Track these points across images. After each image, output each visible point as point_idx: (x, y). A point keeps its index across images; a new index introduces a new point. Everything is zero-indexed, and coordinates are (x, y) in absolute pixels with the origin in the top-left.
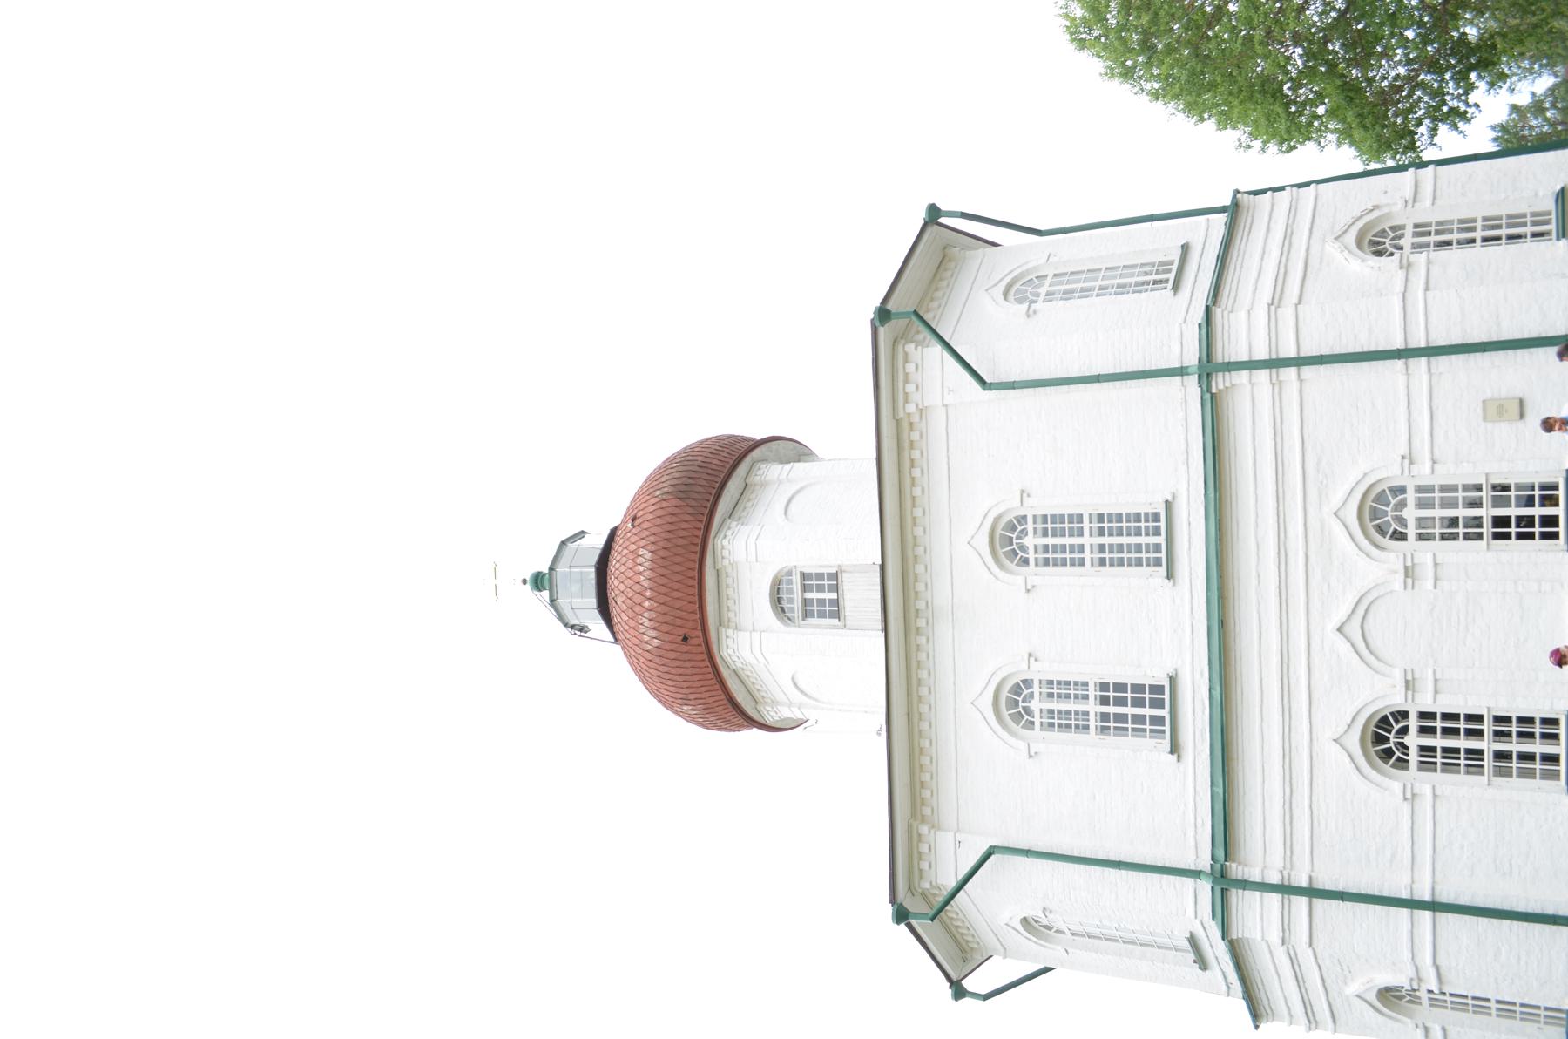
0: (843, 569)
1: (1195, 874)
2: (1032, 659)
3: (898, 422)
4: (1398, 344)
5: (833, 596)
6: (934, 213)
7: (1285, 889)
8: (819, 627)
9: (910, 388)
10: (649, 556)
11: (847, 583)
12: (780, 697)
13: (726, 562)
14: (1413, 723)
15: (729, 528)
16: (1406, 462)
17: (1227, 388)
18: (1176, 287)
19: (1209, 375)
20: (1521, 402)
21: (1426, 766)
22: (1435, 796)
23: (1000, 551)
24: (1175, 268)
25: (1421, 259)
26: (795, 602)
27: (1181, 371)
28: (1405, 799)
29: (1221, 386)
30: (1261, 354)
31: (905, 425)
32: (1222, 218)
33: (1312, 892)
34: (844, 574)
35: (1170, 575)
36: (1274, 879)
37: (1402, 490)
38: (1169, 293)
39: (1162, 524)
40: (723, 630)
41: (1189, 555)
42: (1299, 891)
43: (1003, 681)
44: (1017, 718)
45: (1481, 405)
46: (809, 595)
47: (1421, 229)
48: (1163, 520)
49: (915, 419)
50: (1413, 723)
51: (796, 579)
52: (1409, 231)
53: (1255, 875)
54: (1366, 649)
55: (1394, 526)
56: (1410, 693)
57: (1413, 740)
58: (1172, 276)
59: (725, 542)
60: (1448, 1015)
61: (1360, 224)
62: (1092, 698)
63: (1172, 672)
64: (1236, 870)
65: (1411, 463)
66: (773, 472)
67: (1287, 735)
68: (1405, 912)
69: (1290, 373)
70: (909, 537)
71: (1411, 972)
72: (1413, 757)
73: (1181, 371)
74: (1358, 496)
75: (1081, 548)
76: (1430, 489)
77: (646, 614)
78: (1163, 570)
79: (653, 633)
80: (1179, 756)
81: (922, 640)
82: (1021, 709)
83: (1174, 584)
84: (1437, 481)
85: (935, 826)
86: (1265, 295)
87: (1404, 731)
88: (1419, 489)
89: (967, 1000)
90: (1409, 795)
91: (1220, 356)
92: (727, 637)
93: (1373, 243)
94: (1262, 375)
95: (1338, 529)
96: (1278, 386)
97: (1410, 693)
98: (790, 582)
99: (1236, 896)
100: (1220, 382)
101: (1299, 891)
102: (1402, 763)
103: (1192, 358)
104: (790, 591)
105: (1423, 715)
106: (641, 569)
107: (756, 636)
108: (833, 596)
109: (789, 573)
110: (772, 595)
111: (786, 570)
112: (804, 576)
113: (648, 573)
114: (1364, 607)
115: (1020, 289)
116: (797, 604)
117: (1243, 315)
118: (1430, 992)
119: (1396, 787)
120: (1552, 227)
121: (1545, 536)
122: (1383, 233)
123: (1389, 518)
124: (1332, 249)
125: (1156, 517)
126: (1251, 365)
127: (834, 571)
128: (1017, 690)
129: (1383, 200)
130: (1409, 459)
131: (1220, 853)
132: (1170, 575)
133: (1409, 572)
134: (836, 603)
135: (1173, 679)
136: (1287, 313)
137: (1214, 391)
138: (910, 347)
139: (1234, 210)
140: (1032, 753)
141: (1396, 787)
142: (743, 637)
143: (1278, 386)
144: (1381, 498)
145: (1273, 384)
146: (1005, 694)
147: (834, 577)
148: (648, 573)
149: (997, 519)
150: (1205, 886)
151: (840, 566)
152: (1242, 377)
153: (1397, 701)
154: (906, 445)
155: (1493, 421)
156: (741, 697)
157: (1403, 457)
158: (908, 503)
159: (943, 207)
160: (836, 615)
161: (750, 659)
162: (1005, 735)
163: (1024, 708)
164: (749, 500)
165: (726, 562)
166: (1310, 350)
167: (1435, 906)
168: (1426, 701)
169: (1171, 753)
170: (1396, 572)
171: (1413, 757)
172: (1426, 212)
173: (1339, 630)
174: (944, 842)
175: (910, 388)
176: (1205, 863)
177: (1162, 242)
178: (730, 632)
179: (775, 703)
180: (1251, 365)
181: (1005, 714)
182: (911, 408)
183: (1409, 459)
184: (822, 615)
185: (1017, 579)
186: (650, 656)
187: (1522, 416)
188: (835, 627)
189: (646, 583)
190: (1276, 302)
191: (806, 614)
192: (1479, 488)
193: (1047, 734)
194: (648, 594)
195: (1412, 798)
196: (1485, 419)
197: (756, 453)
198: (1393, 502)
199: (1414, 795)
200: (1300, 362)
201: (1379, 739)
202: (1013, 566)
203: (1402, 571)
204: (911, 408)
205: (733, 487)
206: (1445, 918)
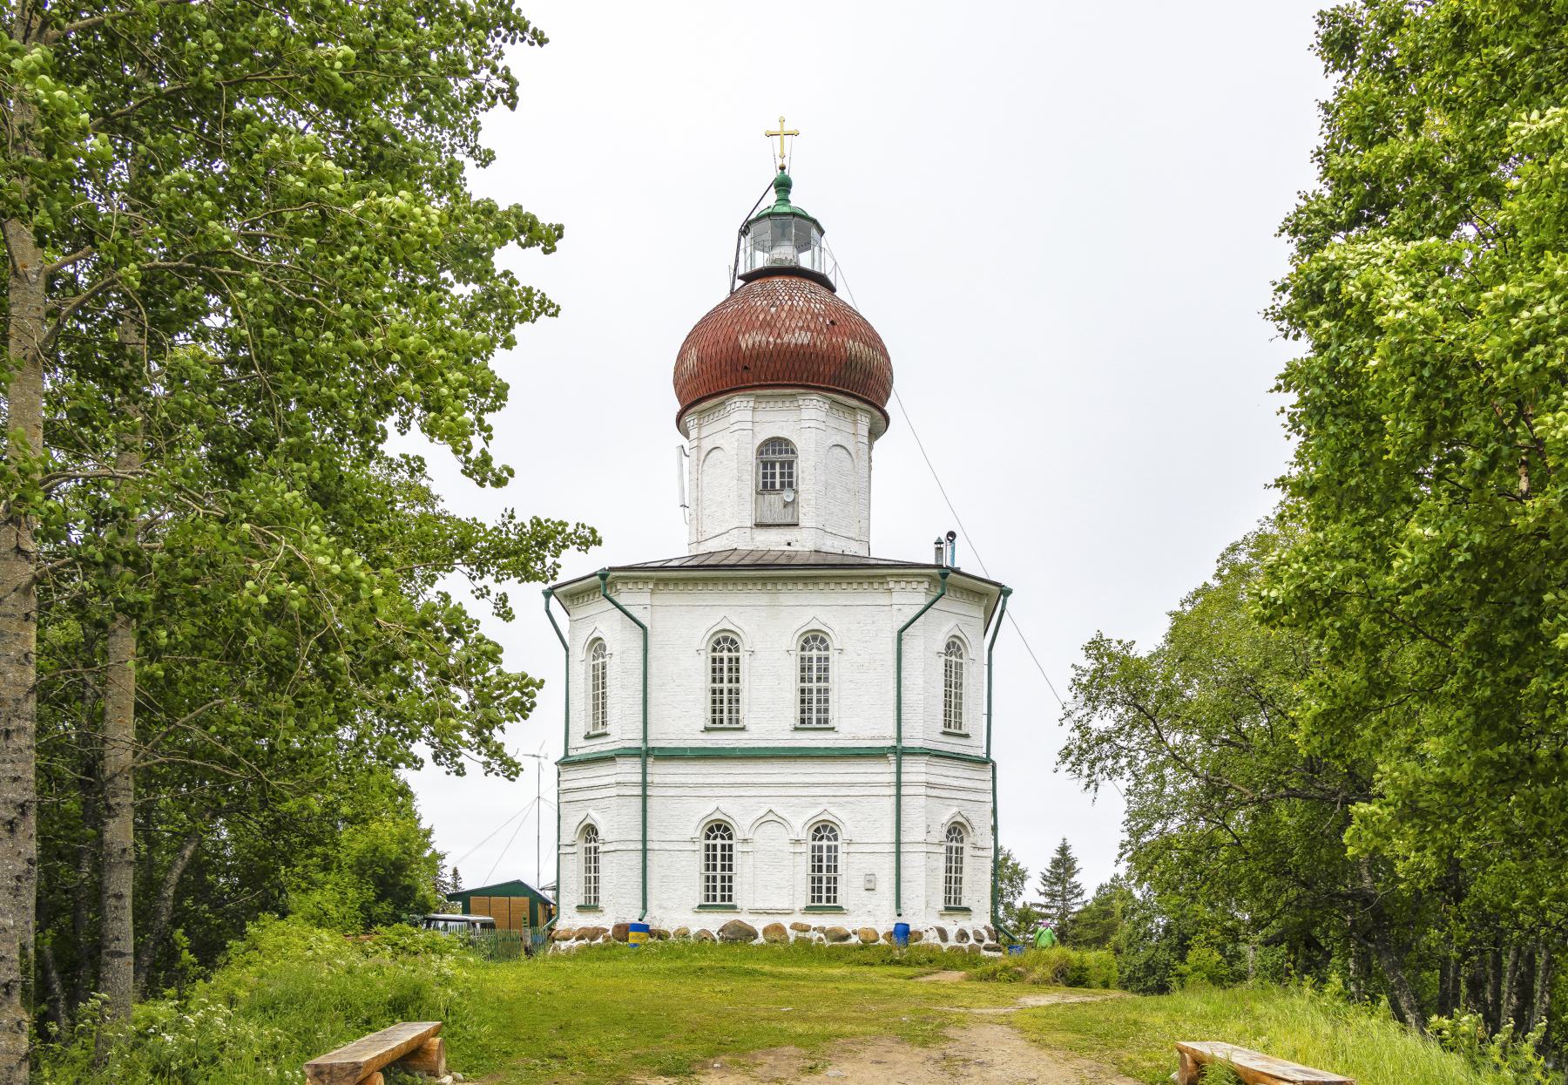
1: (645, 739)
3: (884, 576)
4: (903, 839)
5: (778, 486)
6: (1006, 592)
7: (644, 785)
8: (757, 474)
10: (806, 342)
12: (705, 431)
18: (944, 733)
23: (809, 635)
24: (957, 731)
25: (943, 849)
27: (899, 739)
30: (904, 778)
32: (982, 753)
33: (645, 797)
36: (649, 779)
37: (836, 839)
38: (943, 729)
39: (823, 726)
42: (644, 790)
47: (960, 850)
48: (824, 725)
50: (727, 842)
52: (959, 845)
53: (649, 770)
54: (761, 822)
57: (719, 842)
58: (952, 730)
60: (582, 856)
61: (965, 823)
64: (650, 760)
66: (863, 428)
67: (717, 785)
68: (640, 838)
69: (893, 791)
71: (607, 840)
72: (711, 842)
73: (899, 739)
74: (831, 819)
76: (836, 851)
79: (750, 343)
84: (839, 854)
85: (652, 592)
86: (932, 779)
88: (836, 847)
89: (543, 599)
93: (955, 829)
94: (893, 778)
96: (888, 785)
98: (787, 452)
99: (638, 761)
100: (892, 758)
101: (644, 790)
102: (708, 837)
103: (905, 743)
104: (780, 452)
105: (730, 847)
107: (749, 426)
108: (778, 486)
109: (793, 452)
110: (779, 438)
112: (790, 465)
114: (781, 821)
115: (954, 647)
116: (771, 457)
117: (924, 770)
119: (697, 834)
120: (952, 905)
121: (813, 897)
122: (960, 833)
124: (955, 810)
125: (826, 721)
126: (899, 773)
128: (733, 642)
129: (978, 831)
130: (850, 843)
131: (656, 753)
132: (796, 729)
133: (798, 841)
135: (743, 729)
136: (922, 790)
139: (985, 762)
141: (697, 834)
142: (748, 415)
143: (888, 785)
144: (832, 830)
146: (731, 636)
150: (639, 744)
152: (893, 768)
153: (738, 834)
159: (1009, 599)
160: (765, 484)
161: (735, 417)
162: (708, 636)
166: (904, 800)
167: (645, 851)
171: (711, 842)
172: (968, 851)
174: (645, 598)
176: (651, 744)
177: (973, 720)
178: (752, 404)
179: (700, 426)
180: (899, 773)
181: (720, 635)
183: (850, 843)
186: (733, 338)
190: (929, 785)
192: (835, 871)
193: (710, 660)
195: (692, 841)
197: (877, 413)
200: (899, 796)
202: (801, 642)
205: (854, 403)
206: (638, 857)
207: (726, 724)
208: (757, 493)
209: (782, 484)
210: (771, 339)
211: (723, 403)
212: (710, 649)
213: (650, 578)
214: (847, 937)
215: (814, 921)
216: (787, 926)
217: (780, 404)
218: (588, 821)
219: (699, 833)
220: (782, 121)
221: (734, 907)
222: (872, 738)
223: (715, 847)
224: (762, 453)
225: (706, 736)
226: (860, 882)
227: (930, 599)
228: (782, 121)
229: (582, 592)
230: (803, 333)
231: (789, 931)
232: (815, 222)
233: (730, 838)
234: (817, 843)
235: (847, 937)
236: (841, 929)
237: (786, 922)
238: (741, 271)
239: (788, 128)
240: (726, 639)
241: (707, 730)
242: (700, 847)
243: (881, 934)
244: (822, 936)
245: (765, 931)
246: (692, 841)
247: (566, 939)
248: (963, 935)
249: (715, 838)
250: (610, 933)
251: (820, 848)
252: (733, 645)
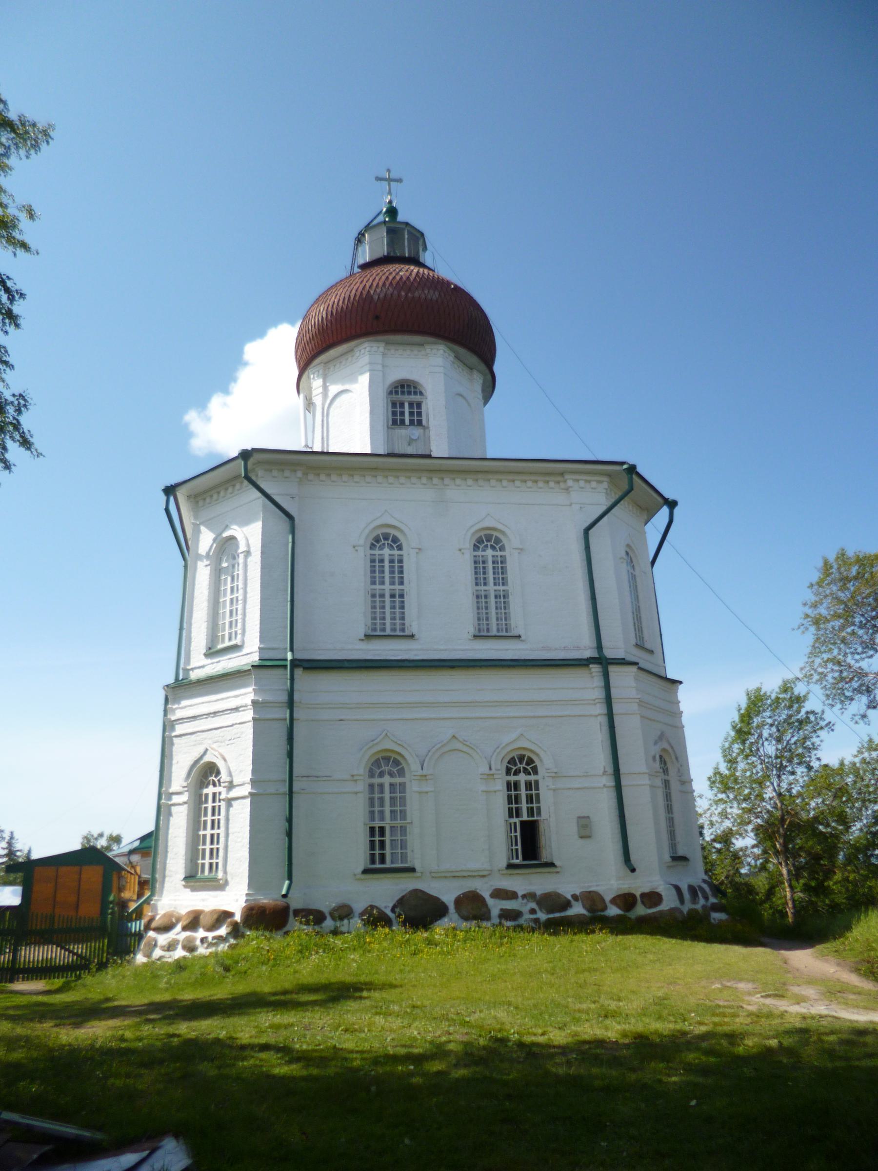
0: (427, 430)
2: (417, 550)
5: (407, 422)
8: (387, 409)
9: (582, 483)
10: (434, 298)
11: (416, 432)
13: (428, 351)
14: (397, 780)
15: (449, 355)
16: (553, 775)
17: (591, 673)
19: (600, 663)
20: (589, 837)
21: (371, 786)
22: (356, 793)
26: (402, 397)
28: (353, 776)
29: (593, 670)
31: (559, 478)
34: (422, 431)
35: (474, 636)
40: (382, 345)
41: (488, 649)
43: (402, 531)
44: (377, 540)
45: (586, 815)
46: (406, 406)
49: (562, 485)
50: (397, 780)
51: (418, 398)
55: (514, 768)
56: (419, 778)
57: (387, 780)
59: (441, 352)
61: (670, 750)
62: (392, 587)
63: (417, 636)
65: (553, 777)
70: (490, 476)
72: (377, 780)
73: (600, 647)
74: (533, 747)
75: (383, 583)
77: (395, 292)
78: (477, 634)
80: (363, 640)
81: (424, 480)
82: (383, 542)
83: (470, 640)
84: (542, 791)
87: (391, 775)
88: (537, 782)
90: (355, 778)
91: (612, 669)
92: (378, 347)
95: (514, 736)
97: (419, 778)
98: (415, 393)
102: (371, 774)
104: (409, 393)
105: (403, 785)
106: (426, 292)
108: (407, 422)
109: (421, 393)
110: (407, 380)
111: (423, 391)
112: (419, 405)
113: (423, 296)
118: (220, 793)
123: (519, 765)
126: (607, 687)
127: (424, 422)
128: (395, 540)
130: (556, 776)
134: (403, 422)
137: (591, 666)
138: (605, 485)
140: (356, 548)
145: (594, 700)
146: (393, 532)
147: (420, 423)
148: (423, 296)
149: (503, 533)
151: (428, 428)
152: (598, 682)
154: (547, 478)
155: (578, 823)
156: (333, 353)
157: (556, 773)
158: (511, 477)
160: (394, 422)
163: (384, 544)
164: (463, 370)
165: (428, 351)
168: (413, 787)
169: (365, 636)
170: (490, 769)
171: (377, 780)
173: (454, 736)
175: (582, 483)
178: (381, 349)
180: (607, 687)
182: (570, 483)
183: (556, 776)
184: (394, 413)
185: (468, 545)
187: (582, 837)
188: (388, 422)
189: (417, 294)
191: (394, 405)
193: (368, 558)
194: (410, 295)
195: (354, 779)
196: (579, 817)
198: (528, 767)
199: (356, 781)
201: (387, 759)
202: (473, 541)
203: (492, 772)
204: (570, 483)
207: (388, 631)
208: (388, 428)
209: (412, 422)
210: (403, 294)
211: (352, 350)
212: (369, 545)
213: (299, 464)
214: (567, 905)
215: (520, 883)
216: (486, 895)
217: (408, 352)
218: (207, 758)
219: (361, 770)
220: (389, 171)
221: (412, 870)
222: (565, 649)
223: (381, 786)
224: (391, 393)
225: (364, 646)
226: (572, 828)
227: (609, 504)
228: (389, 171)
229: (205, 492)
230: (431, 291)
231: (490, 902)
232: (422, 235)
233: (401, 773)
234: (512, 778)
235: (567, 905)
236: (558, 895)
237: (485, 891)
238: (361, 261)
239: (393, 176)
240: (386, 537)
241: (368, 637)
242: (361, 786)
243: (608, 898)
244: (533, 905)
245: (458, 902)
246: (354, 779)
247: (166, 928)
248: (693, 890)
249: (381, 775)
250: (238, 918)
251: (516, 785)
252: (396, 543)
